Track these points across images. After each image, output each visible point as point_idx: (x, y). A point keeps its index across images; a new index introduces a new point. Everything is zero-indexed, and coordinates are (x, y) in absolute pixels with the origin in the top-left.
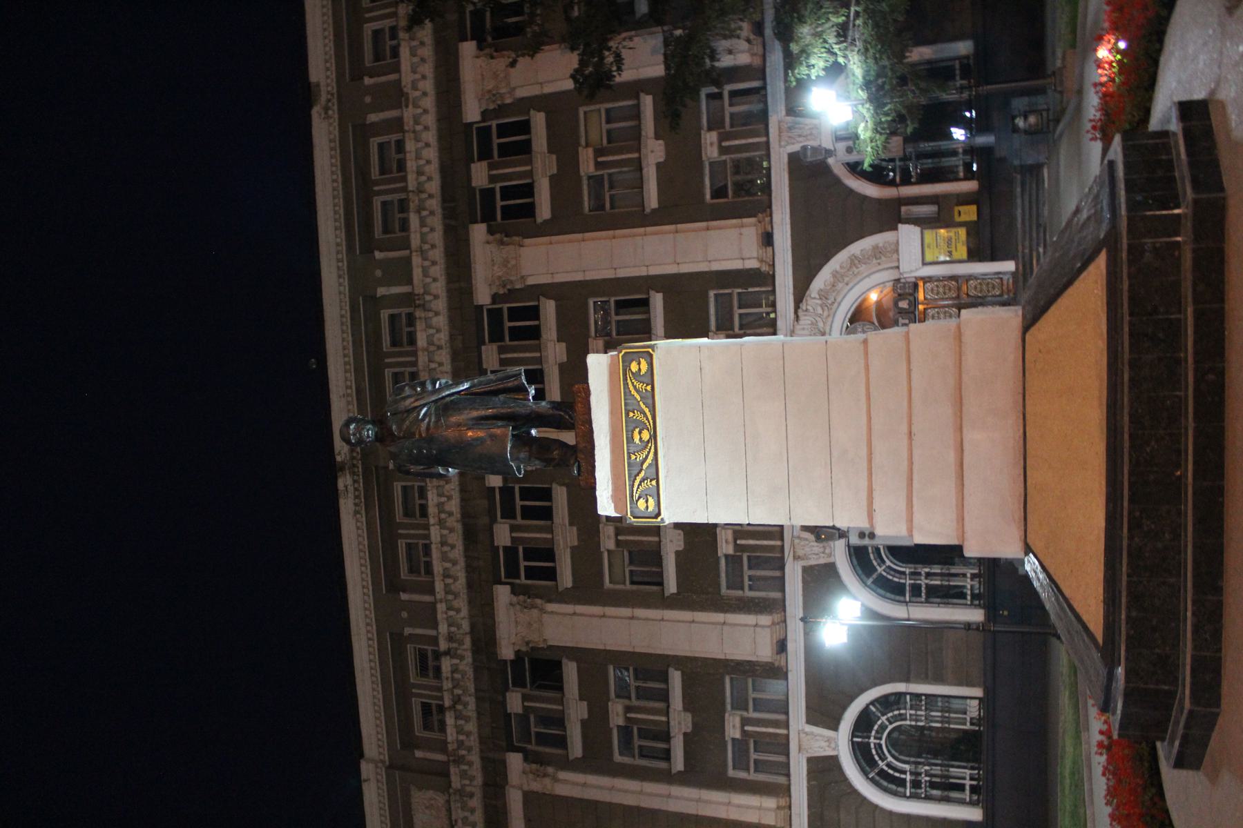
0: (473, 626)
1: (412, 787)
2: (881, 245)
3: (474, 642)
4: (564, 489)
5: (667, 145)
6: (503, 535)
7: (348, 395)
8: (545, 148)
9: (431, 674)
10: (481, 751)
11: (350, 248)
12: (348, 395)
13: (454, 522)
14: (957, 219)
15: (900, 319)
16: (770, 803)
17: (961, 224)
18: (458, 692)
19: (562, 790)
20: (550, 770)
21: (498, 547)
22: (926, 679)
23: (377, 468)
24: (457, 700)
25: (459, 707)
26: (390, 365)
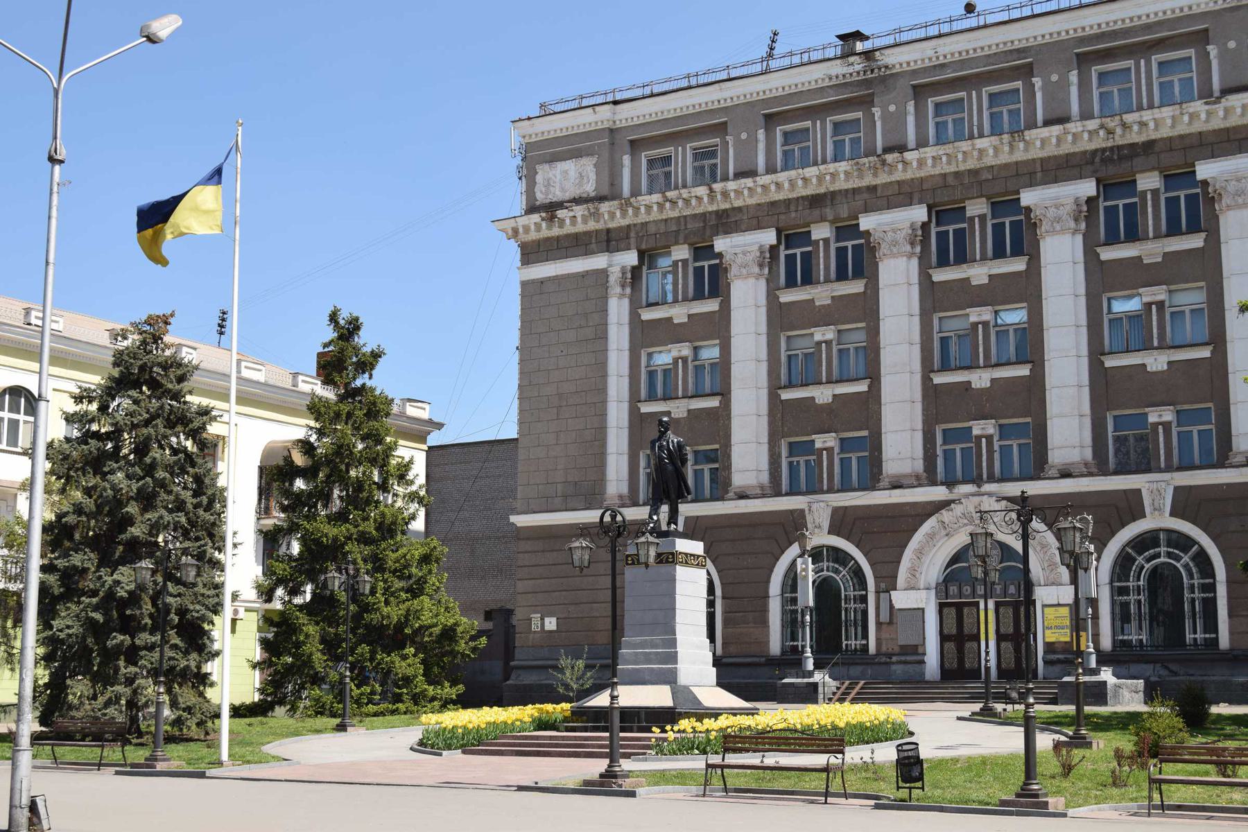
0: (739, 209)
1: (594, 159)
3: (725, 211)
4: (862, 289)
5: (1163, 372)
7: (938, 58)
8: (1168, 249)
9: (696, 164)
10: (635, 225)
11: (1082, 41)
12: (938, 58)
13: (829, 186)
16: (624, 489)
18: (680, 203)
20: (628, 290)
21: (809, 226)
22: (725, 612)
23: (873, 94)
24: (673, 203)
25: (668, 205)
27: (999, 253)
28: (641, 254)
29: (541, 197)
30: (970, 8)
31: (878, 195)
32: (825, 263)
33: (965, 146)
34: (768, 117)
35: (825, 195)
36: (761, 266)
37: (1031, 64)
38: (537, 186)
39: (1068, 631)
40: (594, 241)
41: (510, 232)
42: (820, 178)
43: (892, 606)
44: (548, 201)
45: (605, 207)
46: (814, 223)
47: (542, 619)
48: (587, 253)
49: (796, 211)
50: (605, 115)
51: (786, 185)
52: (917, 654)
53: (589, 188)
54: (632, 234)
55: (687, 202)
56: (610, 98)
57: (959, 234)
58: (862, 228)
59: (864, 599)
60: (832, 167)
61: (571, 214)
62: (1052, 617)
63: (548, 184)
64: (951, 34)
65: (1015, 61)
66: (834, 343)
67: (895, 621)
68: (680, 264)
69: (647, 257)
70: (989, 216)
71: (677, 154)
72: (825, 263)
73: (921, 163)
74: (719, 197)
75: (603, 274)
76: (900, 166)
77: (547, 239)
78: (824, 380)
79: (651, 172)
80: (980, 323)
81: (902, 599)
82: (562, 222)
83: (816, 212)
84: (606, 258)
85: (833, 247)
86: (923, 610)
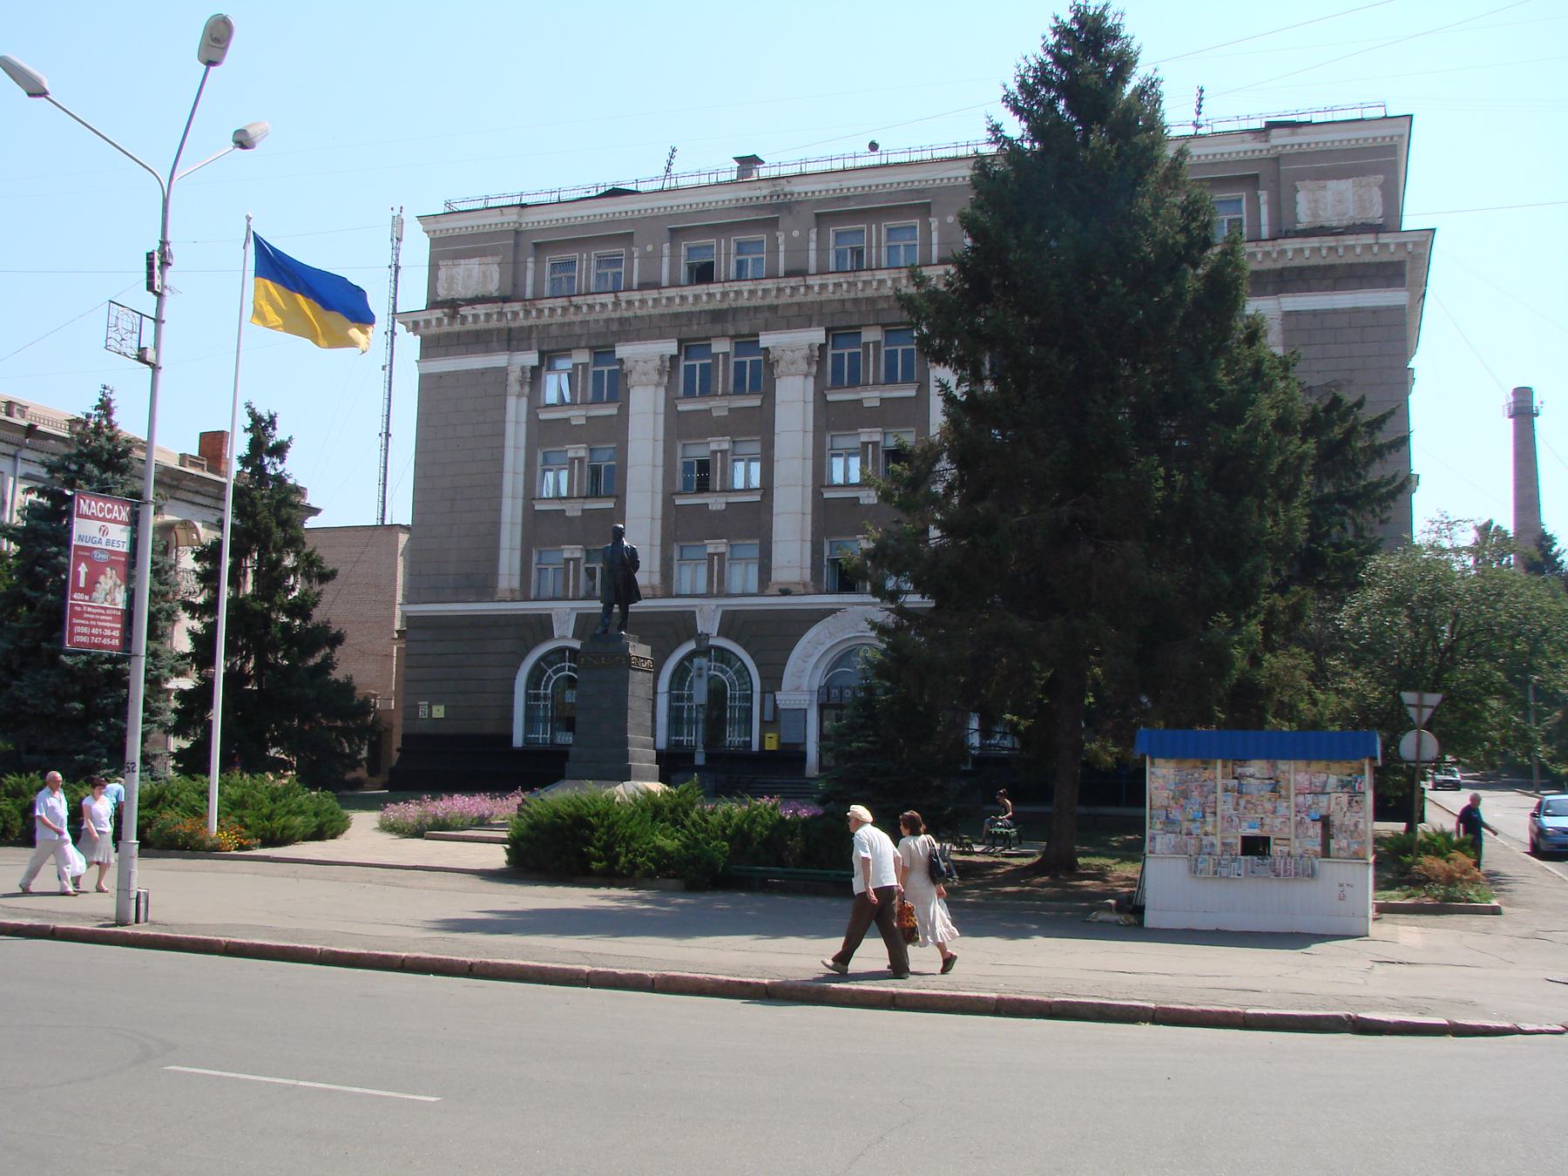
1: (498, 259)
3: (628, 319)
6: (721, 346)
10: (537, 326)
13: (730, 302)
16: (516, 584)
19: (511, 402)
20: (527, 389)
24: (578, 307)
25: (572, 309)
26: (870, 229)
27: (891, 379)
28: (542, 354)
29: (443, 293)
30: (873, 146)
31: (779, 314)
32: (723, 378)
33: (865, 276)
34: (672, 231)
35: (727, 309)
36: (660, 374)
37: (929, 203)
38: (439, 281)
40: (495, 339)
41: (411, 325)
42: (725, 294)
43: (776, 706)
44: (450, 297)
45: (508, 308)
46: (866, 326)
47: (430, 707)
48: (488, 350)
49: (699, 324)
50: (512, 217)
51: (691, 299)
53: (493, 288)
54: (534, 335)
55: (591, 307)
56: (516, 201)
57: (854, 358)
58: (762, 345)
59: (750, 698)
60: (736, 286)
61: (474, 312)
63: (451, 280)
64: (855, 169)
66: (729, 453)
68: (580, 367)
69: (548, 358)
70: (883, 344)
71: (581, 260)
72: (723, 378)
73: (823, 287)
74: (623, 305)
75: (503, 372)
76: (802, 290)
77: (448, 334)
78: (718, 488)
79: (554, 276)
80: (870, 443)
81: (785, 699)
82: (464, 318)
83: (718, 328)
84: (506, 357)
85: (732, 360)
86: (805, 710)
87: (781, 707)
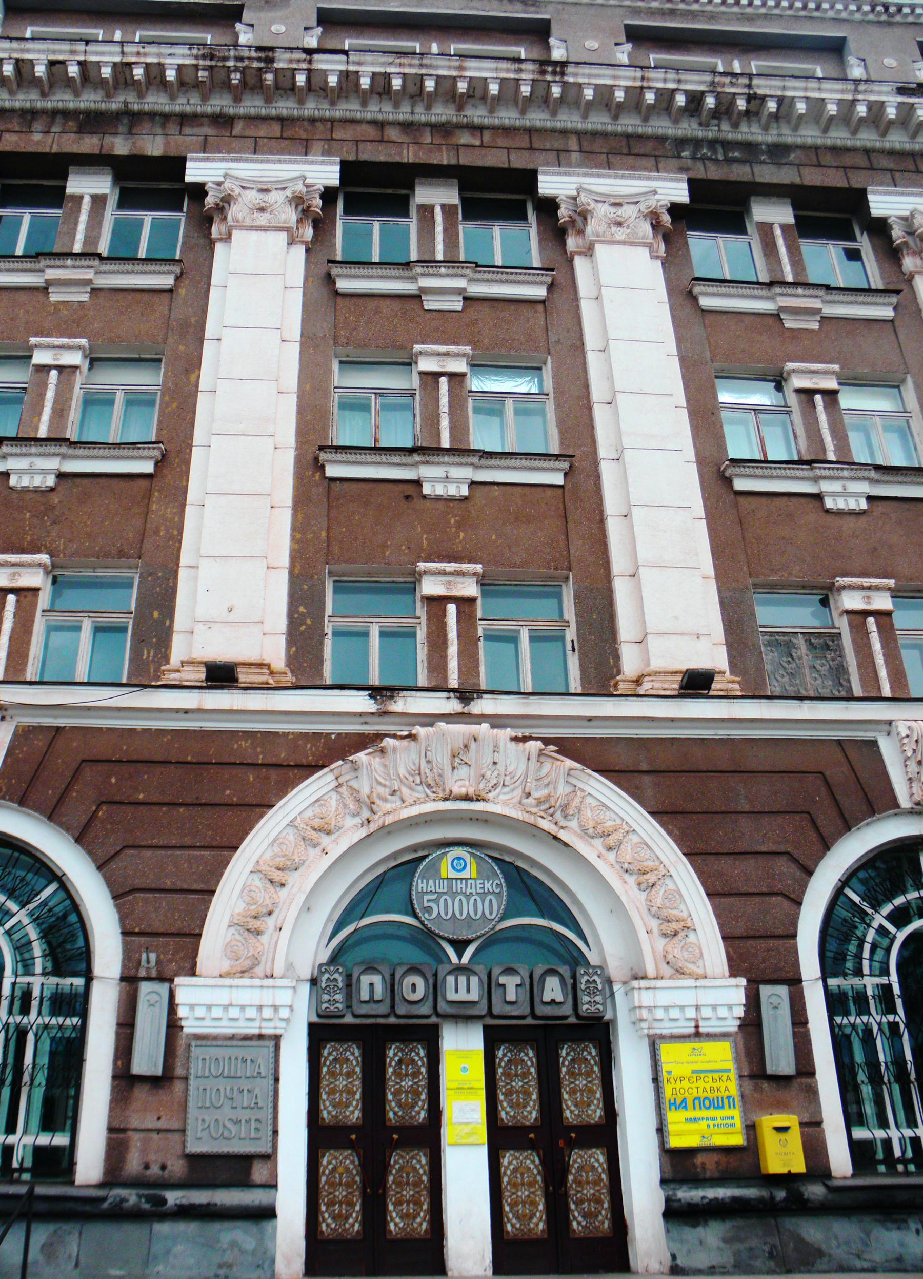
2: (692, 937)
14: (768, 1122)
15: (518, 980)
17: (751, 1129)
31: (234, 133)
39: (736, 1113)
43: (173, 1025)
52: (246, 1183)
62: (686, 1071)
65: (517, 12)
67: (179, 1071)
86: (277, 1038)
87: (190, 1027)
